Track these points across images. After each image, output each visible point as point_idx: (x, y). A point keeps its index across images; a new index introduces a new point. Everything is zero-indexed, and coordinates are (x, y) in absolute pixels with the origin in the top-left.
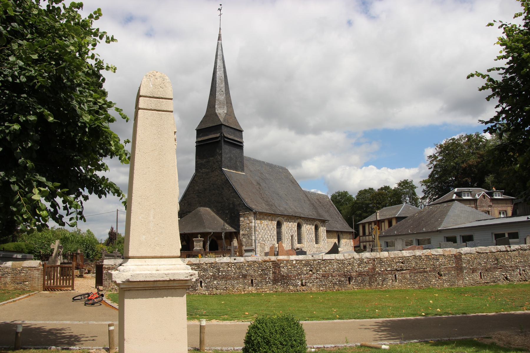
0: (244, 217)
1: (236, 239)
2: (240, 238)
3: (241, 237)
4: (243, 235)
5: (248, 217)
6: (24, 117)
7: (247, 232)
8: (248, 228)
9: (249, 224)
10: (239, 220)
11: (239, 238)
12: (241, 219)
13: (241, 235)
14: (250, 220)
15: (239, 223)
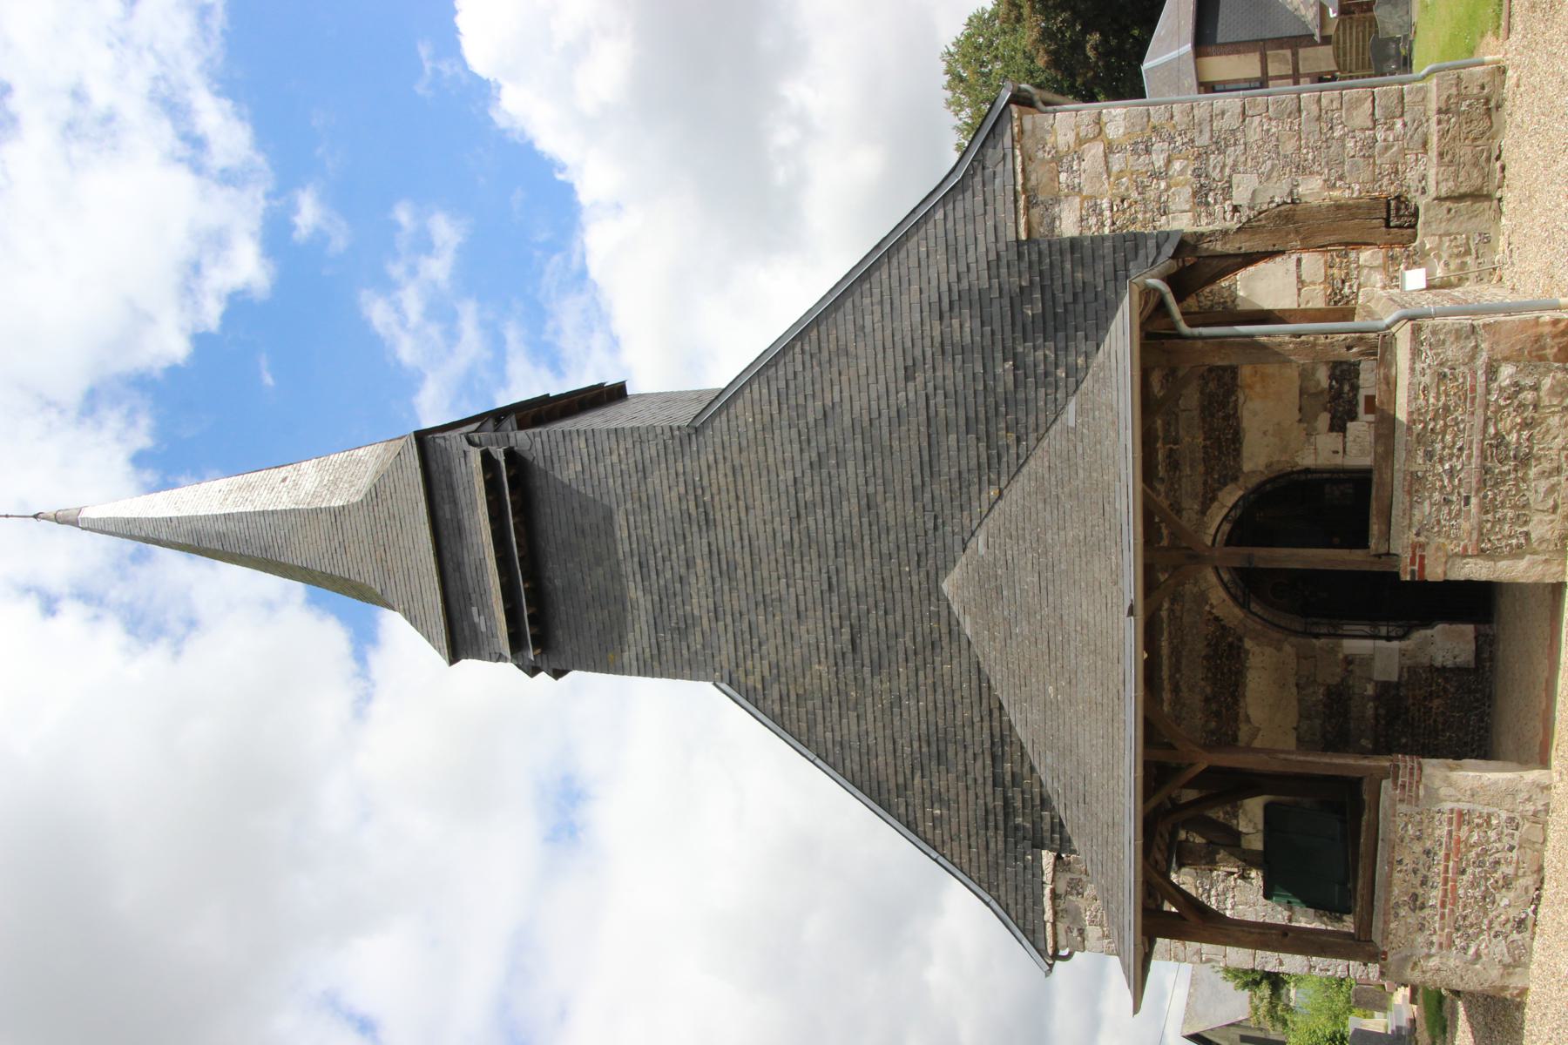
0: (1057, 200)
1: (1241, 275)
2: (1225, 233)
3: (1218, 220)
4: (1200, 196)
5: (1058, 159)
6: (397, 227)
7: (1177, 165)
8: (1148, 151)
9: (1109, 149)
10: (1074, 243)
11: (1231, 248)
12: (1068, 226)
13: (1204, 227)
14: (1081, 141)
15: (1098, 241)
